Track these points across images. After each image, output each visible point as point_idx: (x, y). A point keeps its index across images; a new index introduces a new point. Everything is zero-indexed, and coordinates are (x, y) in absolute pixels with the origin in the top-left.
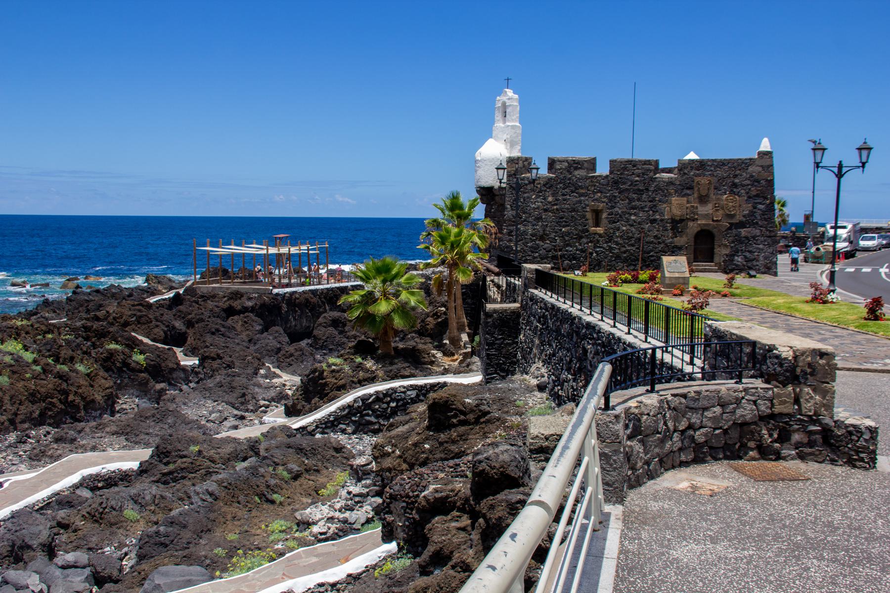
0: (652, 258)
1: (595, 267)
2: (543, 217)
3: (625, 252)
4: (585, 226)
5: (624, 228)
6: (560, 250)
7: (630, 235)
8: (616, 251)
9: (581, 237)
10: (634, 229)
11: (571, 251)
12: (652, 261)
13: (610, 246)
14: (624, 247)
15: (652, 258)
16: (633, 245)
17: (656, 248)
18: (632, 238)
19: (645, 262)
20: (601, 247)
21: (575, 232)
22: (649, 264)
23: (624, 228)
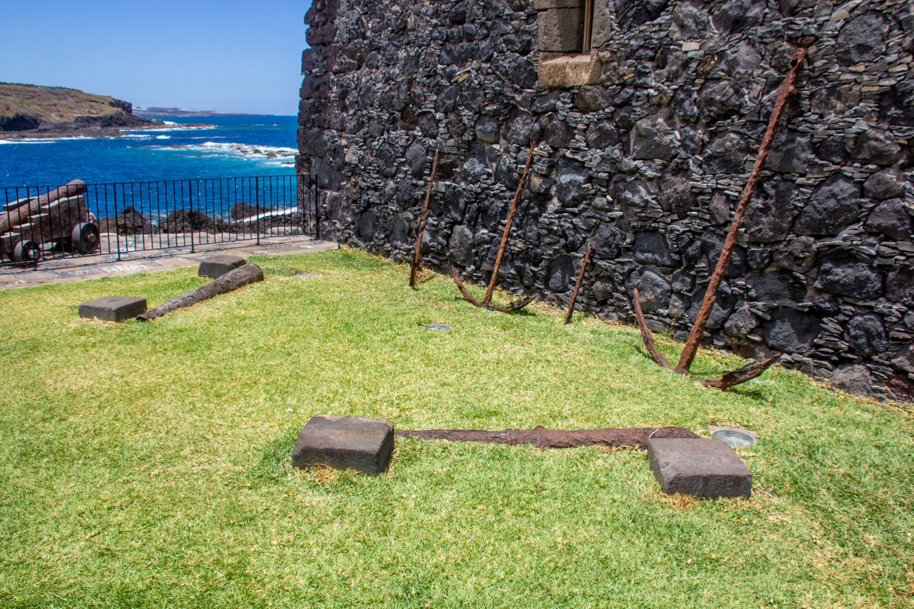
0: (842, 273)
1: (550, 270)
2: (411, 21)
3: (680, 208)
4: (524, 52)
5: (691, 47)
6: (446, 172)
7: (720, 90)
8: (642, 194)
9: (512, 111)
10: (744, 52)
11: (476, 179)
12: (836, 291)
13: (614, 162)
14: (682, 170)
15: (842, 273)
16: (731, 166)
17: (889, 194)
18: (729, 111)
19: (798, 290)
20: (581, 167)
21: (493, 84)
22: (817, 313)
23: (691, 47)
